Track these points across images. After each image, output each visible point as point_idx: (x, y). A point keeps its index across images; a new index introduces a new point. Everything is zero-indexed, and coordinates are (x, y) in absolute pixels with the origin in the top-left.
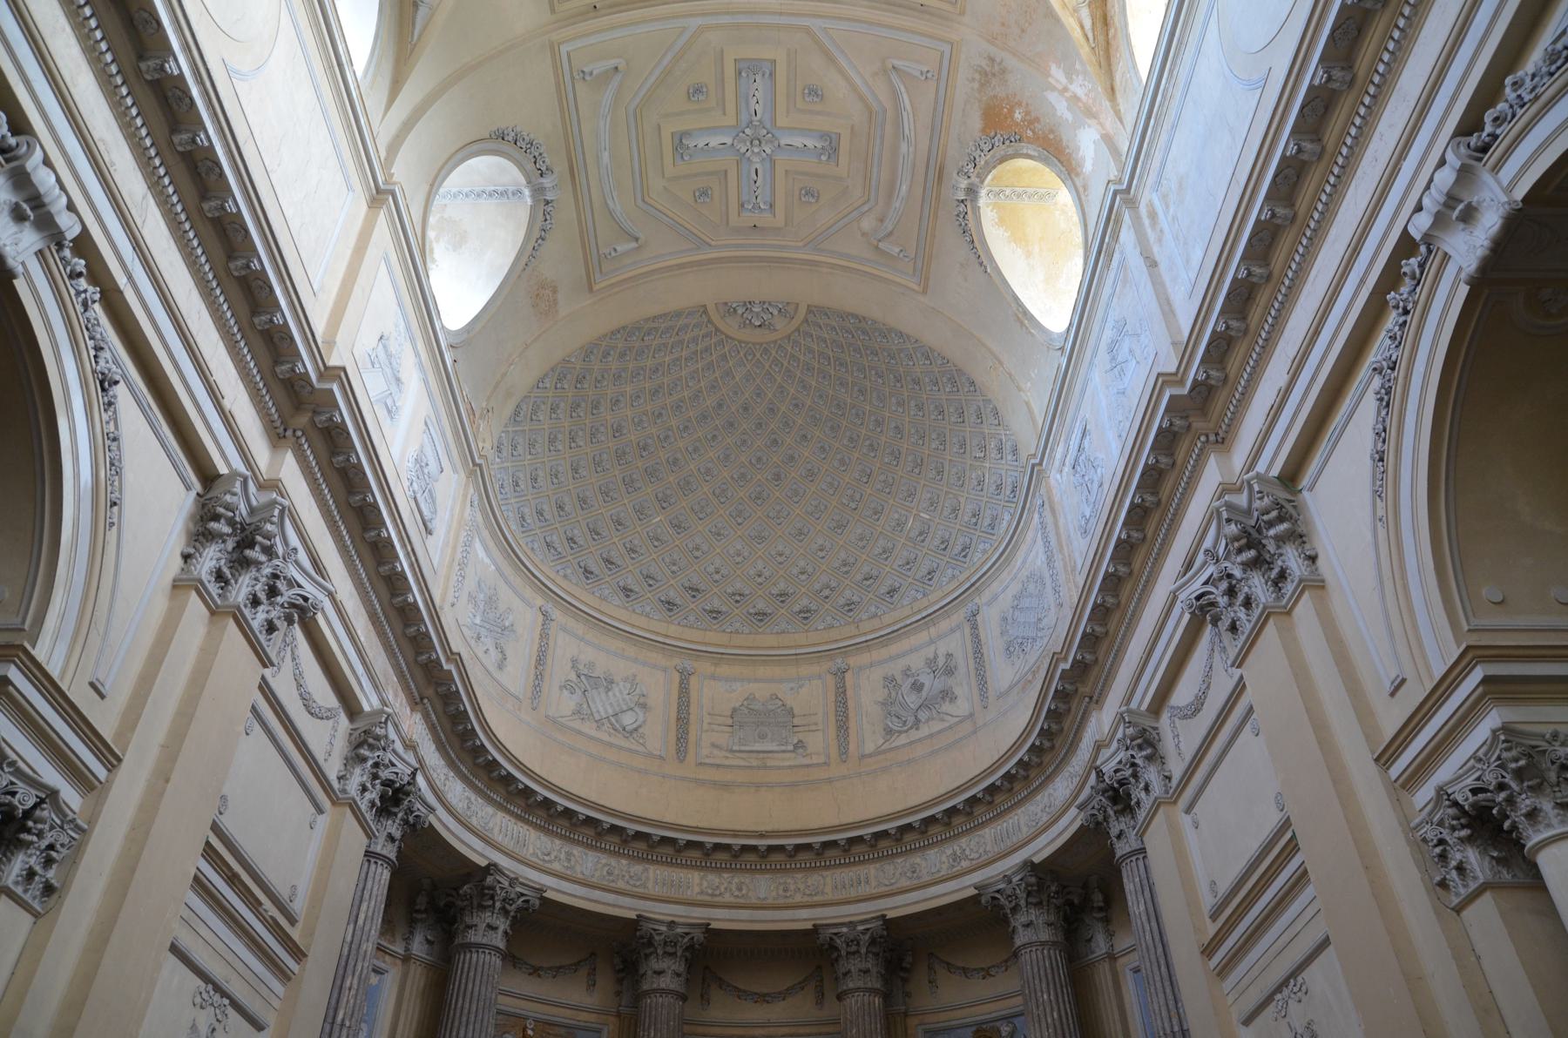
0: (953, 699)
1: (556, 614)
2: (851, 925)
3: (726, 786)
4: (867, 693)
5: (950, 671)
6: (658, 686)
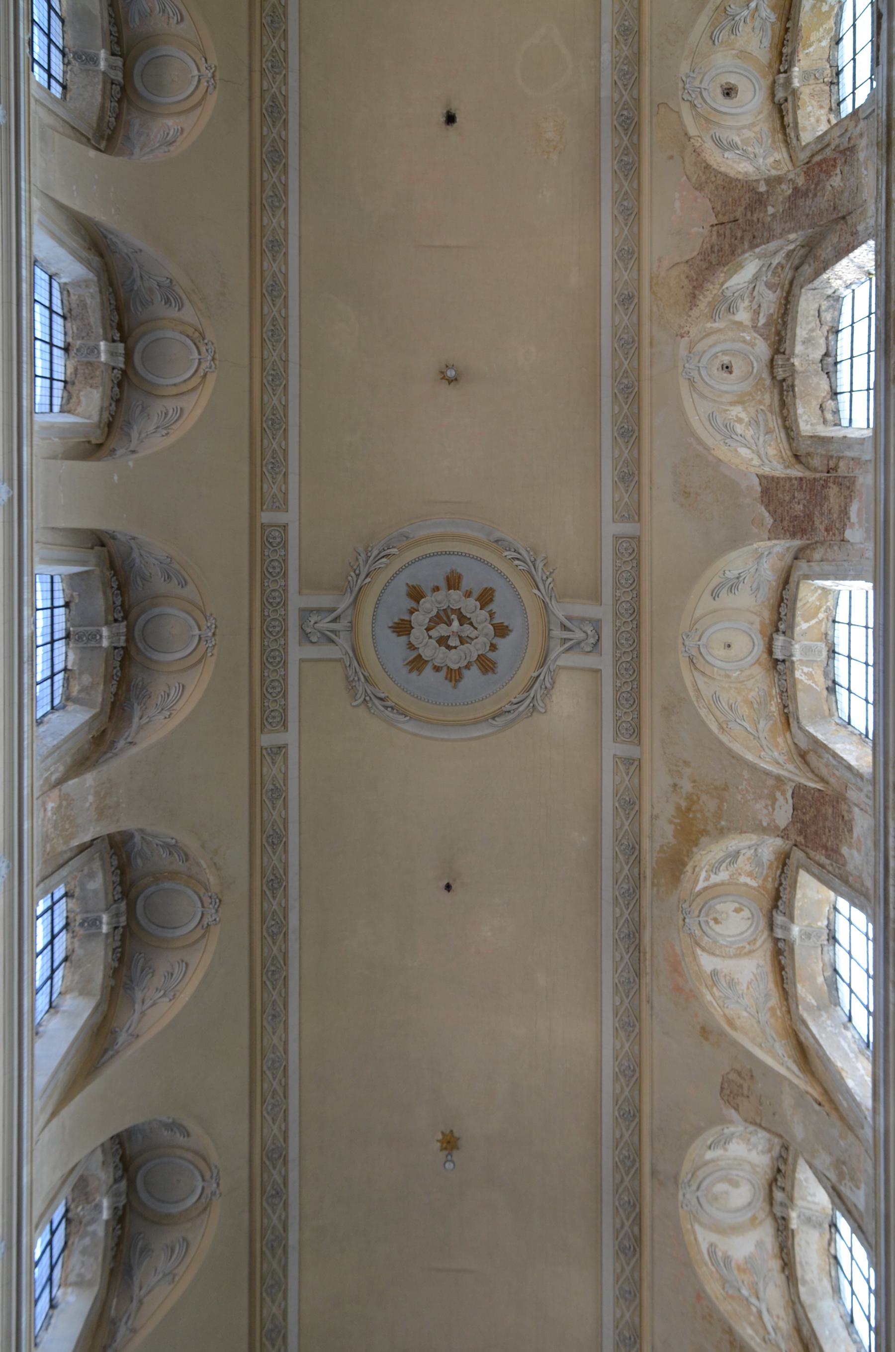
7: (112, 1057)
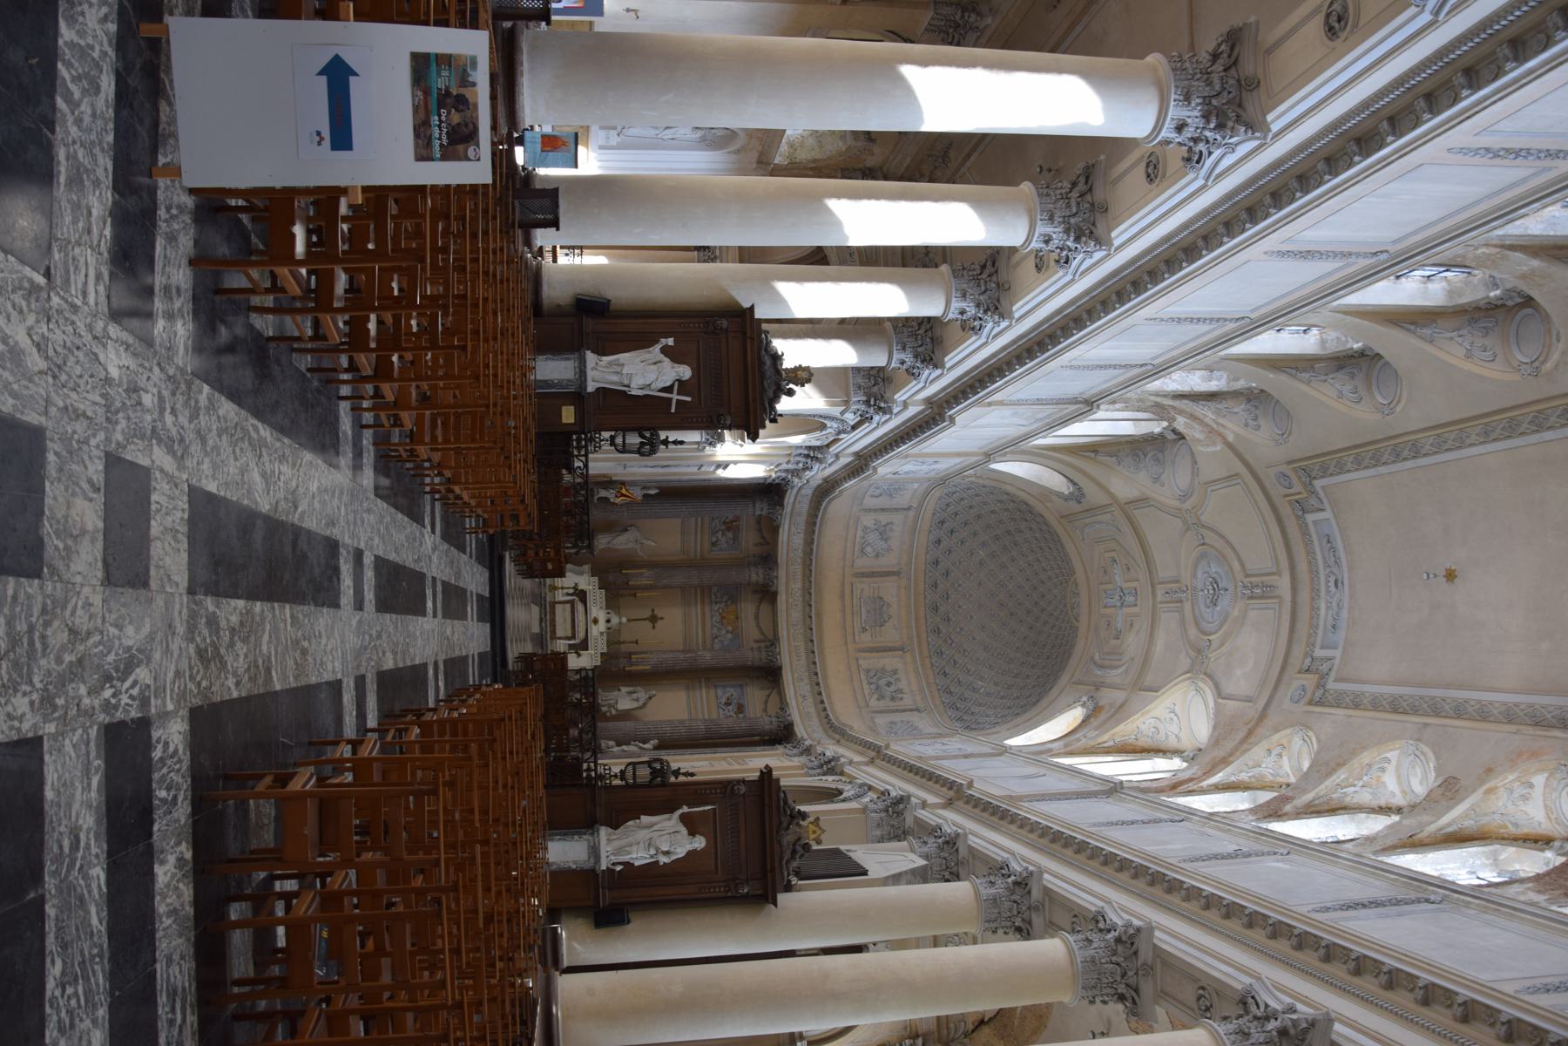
0: (878, 699)
1: (911, 513)
2: (779, 654)
3: (842, 597)
4: (889, 662)
5: (893, 699)
6: (889, 562)
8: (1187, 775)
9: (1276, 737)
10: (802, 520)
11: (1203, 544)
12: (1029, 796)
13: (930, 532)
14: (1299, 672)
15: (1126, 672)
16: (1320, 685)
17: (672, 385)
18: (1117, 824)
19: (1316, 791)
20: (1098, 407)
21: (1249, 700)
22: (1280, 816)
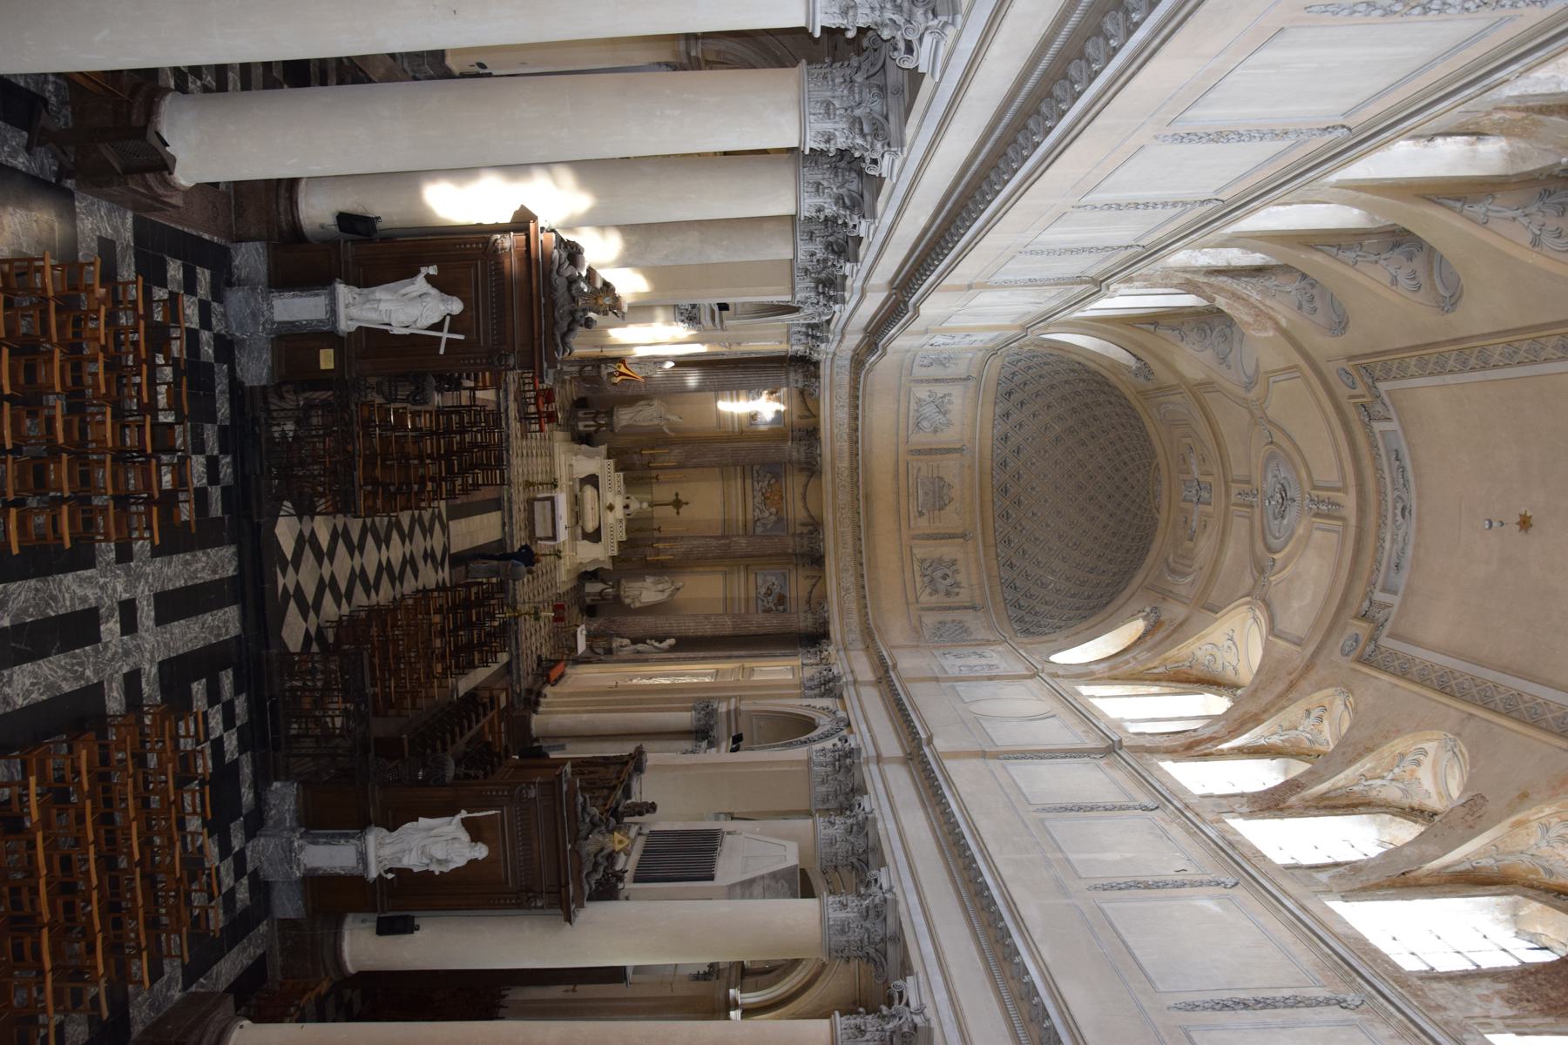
2: (823, 540)
4: (947, 550)
5: (948, 594)
6: (949, 437)
7: (1451, 209)
8: (1207, 733)
9: (1317, 696)
10: (844, 392)
11: (1272, 442)
12: (1006, 752)
13: (996, 403)
14: (1355, 617)
15: (1193, 582)
16: (1373, 638)
17: (443, 321)
18: (1071, 810)
19: (1332, 781)
20: (1108, 287)
21: (1299, 643)
22: (1281, 810)
